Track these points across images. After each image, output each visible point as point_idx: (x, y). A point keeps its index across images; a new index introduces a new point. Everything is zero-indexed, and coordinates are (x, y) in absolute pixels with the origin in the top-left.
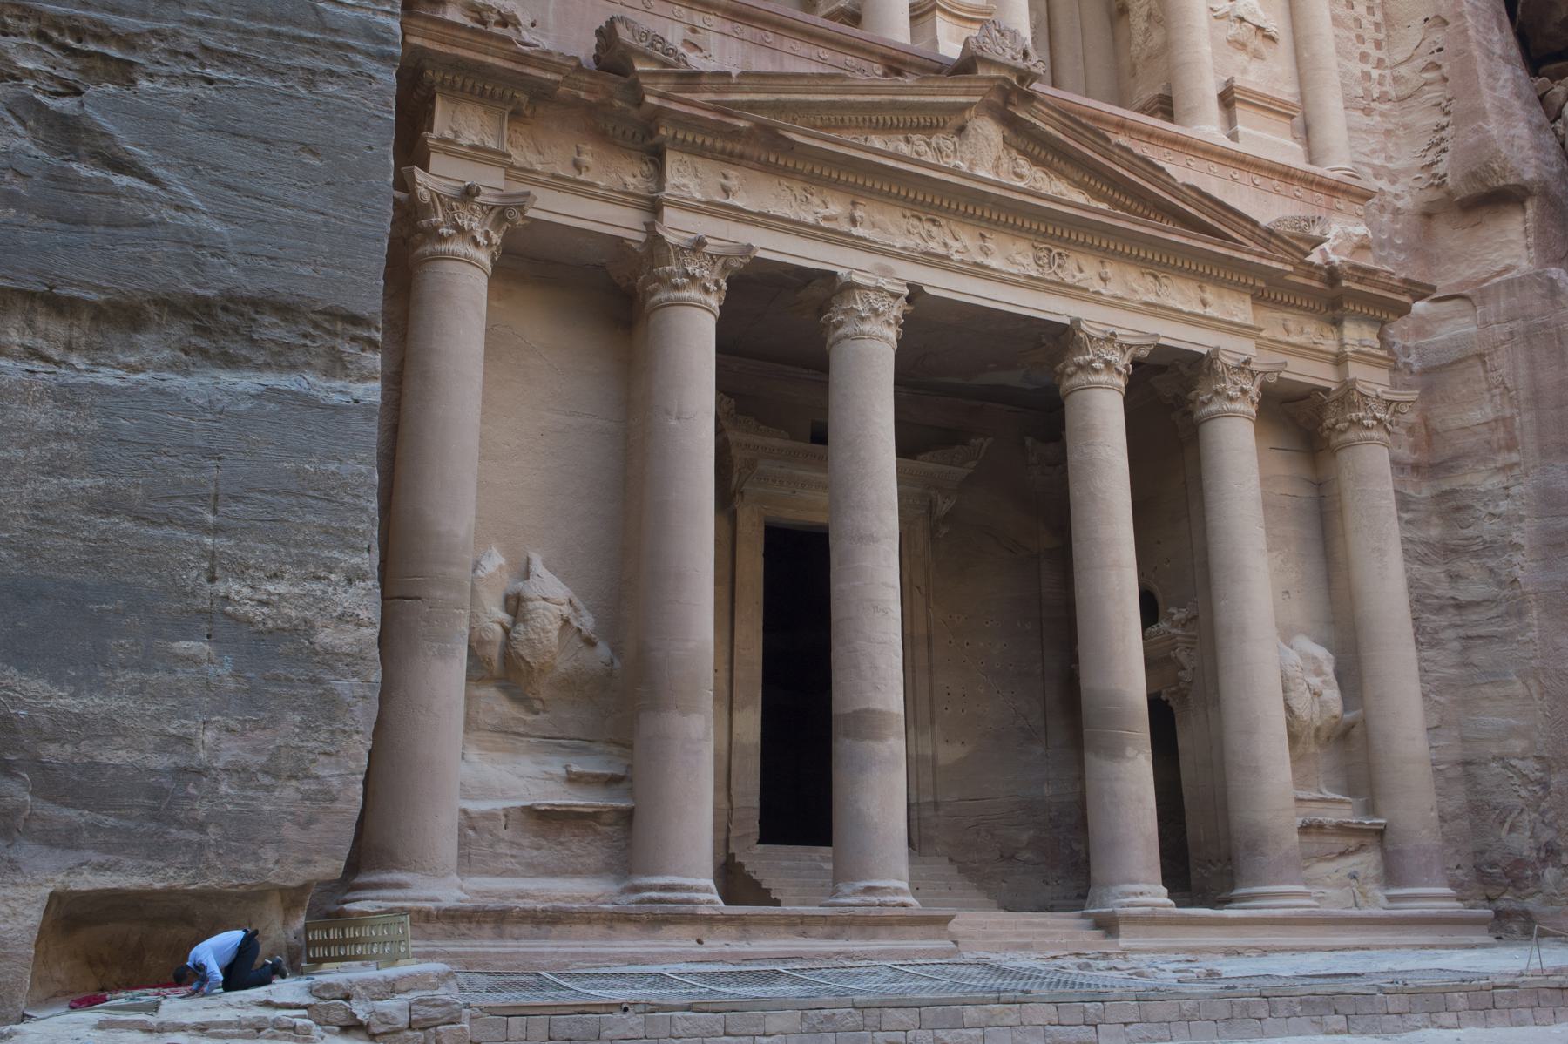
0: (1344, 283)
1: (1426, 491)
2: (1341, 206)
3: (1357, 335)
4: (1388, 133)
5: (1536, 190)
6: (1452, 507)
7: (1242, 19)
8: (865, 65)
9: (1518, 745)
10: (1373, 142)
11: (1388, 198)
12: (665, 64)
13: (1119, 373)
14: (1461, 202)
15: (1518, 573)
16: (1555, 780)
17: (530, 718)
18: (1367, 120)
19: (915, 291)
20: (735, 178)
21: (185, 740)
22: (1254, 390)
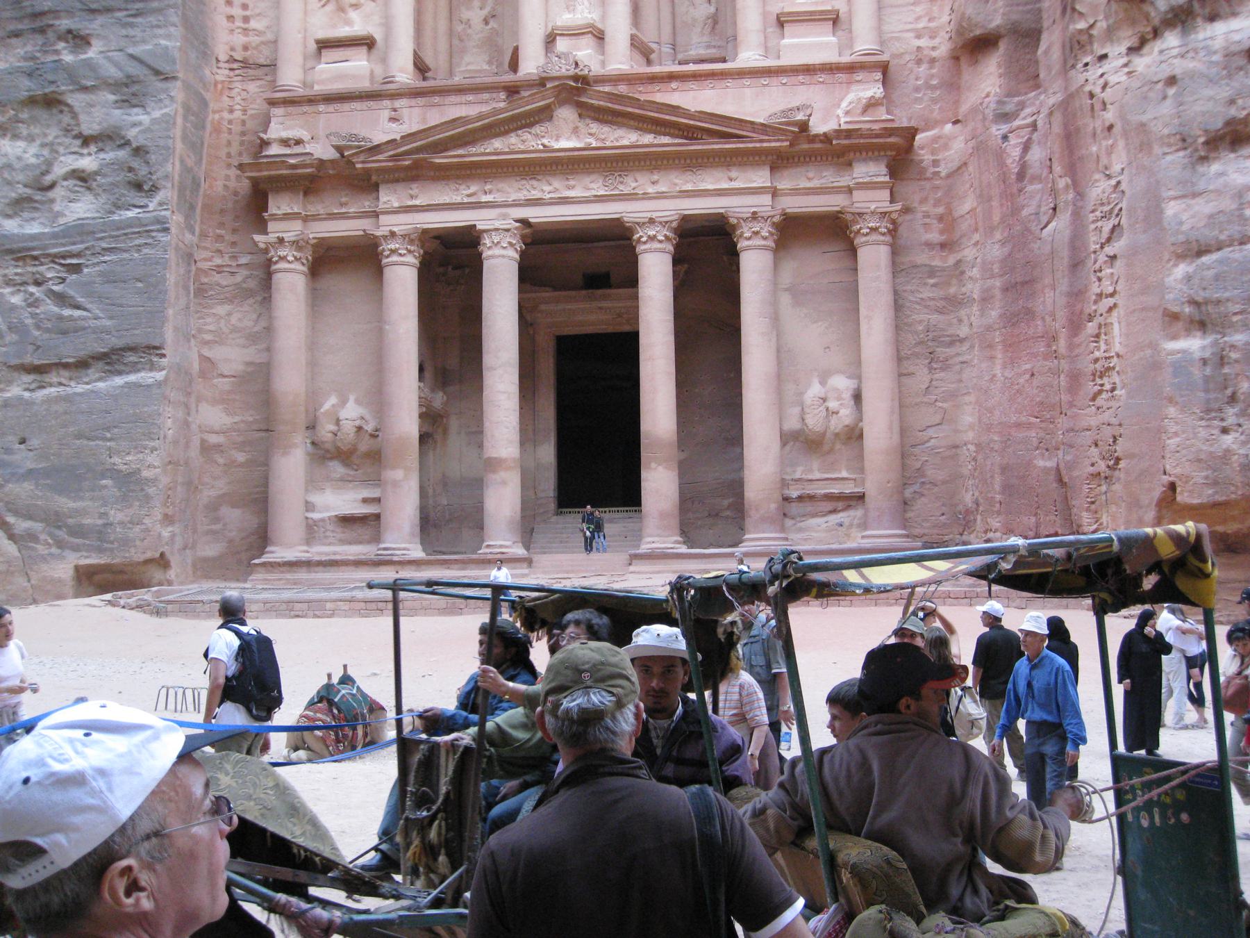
1: (951, 260)
5: (1003, 31)
6: (958, 270)
8: (494, 95)
9: (970, 435)
10: (919, 10)
11: (925, 52)
12: (359, 147)
13: (660, 242)
14: (962, 47)
16: (979, 457)
17: (352, 473)
19: (525, 222)
20: (415, 188)
21: (105, 514)
22: (766, 230)
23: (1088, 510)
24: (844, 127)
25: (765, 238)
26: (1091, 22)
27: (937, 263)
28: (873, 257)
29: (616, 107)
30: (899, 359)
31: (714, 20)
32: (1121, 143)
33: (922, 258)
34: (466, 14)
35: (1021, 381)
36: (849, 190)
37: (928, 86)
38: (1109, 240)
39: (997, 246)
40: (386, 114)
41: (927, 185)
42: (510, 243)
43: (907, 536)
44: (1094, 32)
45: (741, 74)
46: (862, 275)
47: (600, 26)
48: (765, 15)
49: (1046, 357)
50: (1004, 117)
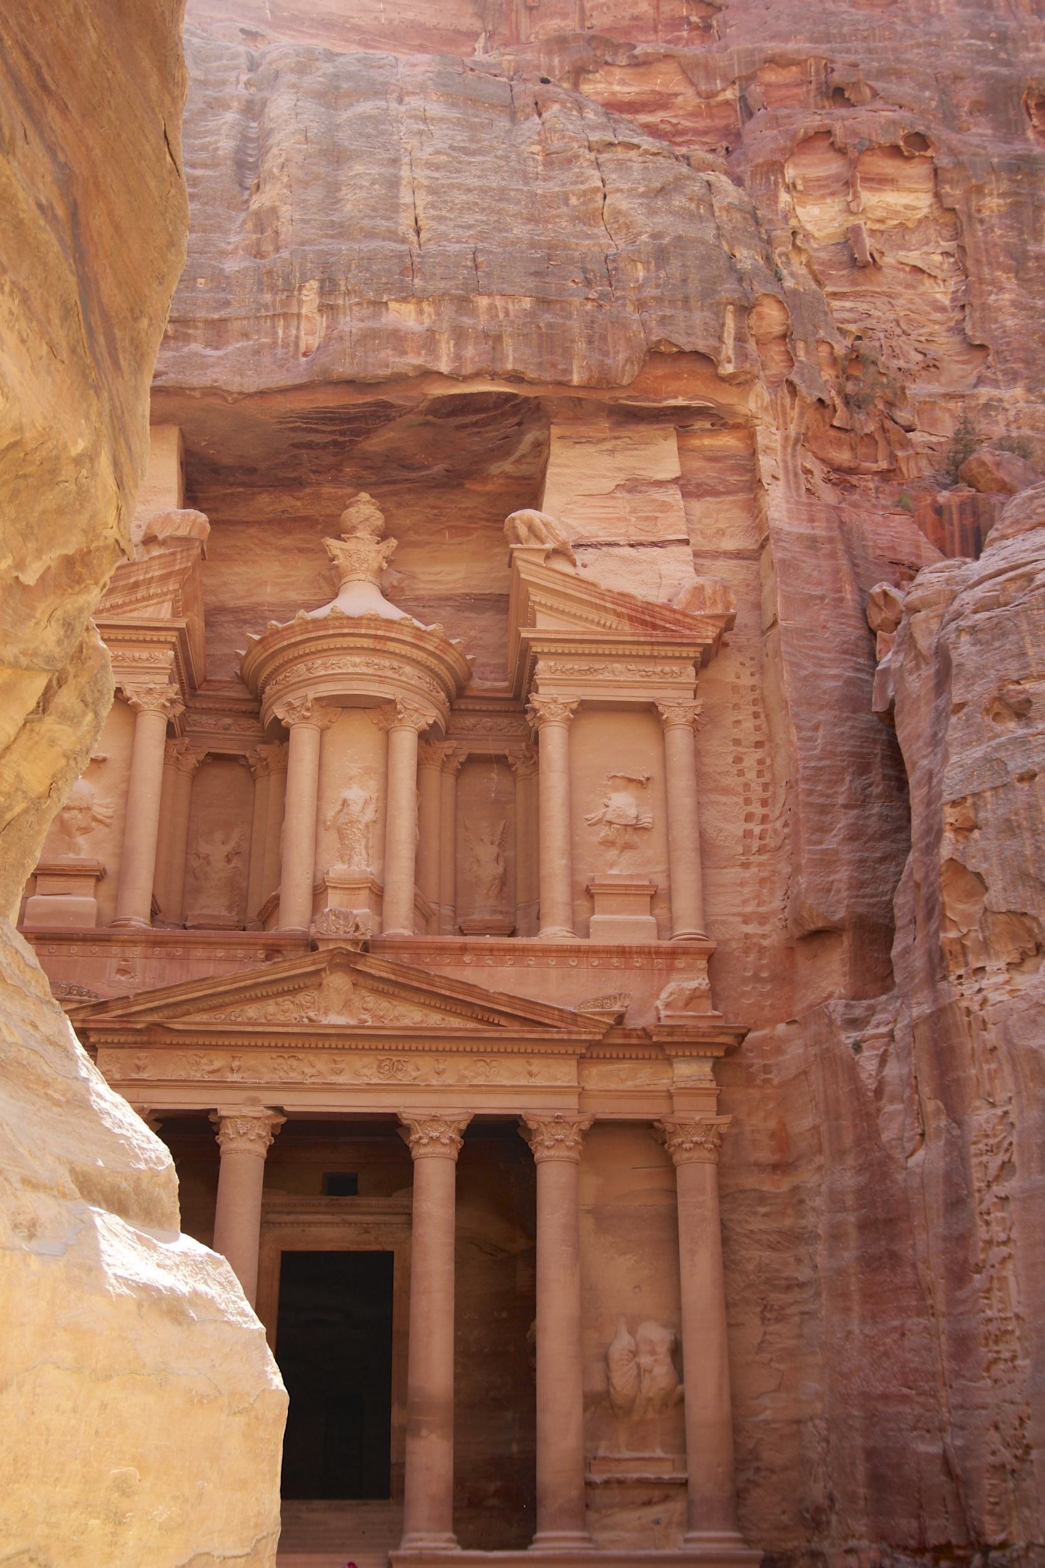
0: (655, 1039)
1: (785, 1186)
2: (682, 966)
3: (691, 1072)
4: (762, 881)
6: (796, 1200)
7: (610, 823)
9: (818, 1407)
10: (747, 891)
11: (755, 940)
12: (81, 1002)
13: (444, 1145)
15: (818, 1259)
16: (833, 1438)
18: (746, 874)
19: (279, 1110)
22: (572, 1138)
23: (991, 1513)
24: (664, 1022)
25: (569, 1148)
26: (965, 931)
27: (767, 1187)
28: (697, 1176)
29: (401, 980)
30: (728, 1305)
31: (503, 881)
32: (1007, 1069)
33: (751, 1181)
34: (204, 848)
35: (888, 1341)
36: (670, 1096)
37: (756, 978)
38: (997, 1178)
39: (849, 1174)
40: (114, 963)
41: (755, 1093)
42: (260, 1136)
43: (746, 1541)
44: (967, 943)
45: (546, 951)
46: (680, 1200)
47: (378, 881)
48: (573, 885)
49: (920, 1313)
50: (854, 1023)
